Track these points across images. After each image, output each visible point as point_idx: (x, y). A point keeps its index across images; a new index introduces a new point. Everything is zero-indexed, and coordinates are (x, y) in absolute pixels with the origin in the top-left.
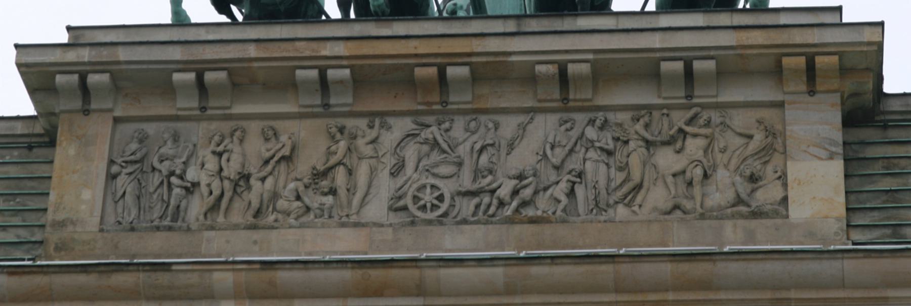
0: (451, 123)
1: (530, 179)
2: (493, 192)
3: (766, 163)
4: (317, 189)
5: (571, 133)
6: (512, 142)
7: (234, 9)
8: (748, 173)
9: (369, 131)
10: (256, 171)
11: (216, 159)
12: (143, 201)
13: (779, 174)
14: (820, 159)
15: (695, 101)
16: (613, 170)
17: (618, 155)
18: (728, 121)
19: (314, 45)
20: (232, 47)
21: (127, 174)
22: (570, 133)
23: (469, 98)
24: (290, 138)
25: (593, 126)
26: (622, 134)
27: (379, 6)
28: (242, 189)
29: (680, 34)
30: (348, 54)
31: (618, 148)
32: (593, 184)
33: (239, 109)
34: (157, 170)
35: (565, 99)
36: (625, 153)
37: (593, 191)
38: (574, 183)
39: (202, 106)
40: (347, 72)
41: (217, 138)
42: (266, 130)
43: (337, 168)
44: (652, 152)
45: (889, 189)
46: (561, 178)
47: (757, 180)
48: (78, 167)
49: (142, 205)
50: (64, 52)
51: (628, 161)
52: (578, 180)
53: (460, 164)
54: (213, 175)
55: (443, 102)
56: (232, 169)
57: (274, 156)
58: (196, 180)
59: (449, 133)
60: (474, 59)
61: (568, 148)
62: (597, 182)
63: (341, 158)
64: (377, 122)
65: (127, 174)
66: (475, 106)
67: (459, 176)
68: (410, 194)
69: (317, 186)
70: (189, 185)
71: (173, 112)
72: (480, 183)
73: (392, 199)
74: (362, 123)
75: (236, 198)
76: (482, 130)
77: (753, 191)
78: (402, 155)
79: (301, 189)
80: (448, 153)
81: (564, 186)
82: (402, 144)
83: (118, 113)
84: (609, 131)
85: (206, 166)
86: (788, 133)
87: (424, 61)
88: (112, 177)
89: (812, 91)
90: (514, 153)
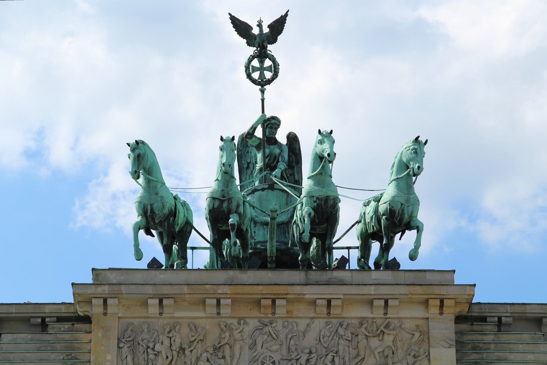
0: (276, 323)
1: (315, 355)
2: (297, 360)
3: (420, 348)
4: (216, 355)
5: (331, 329)
6: (304, 334)
7: (154, 232)
8: (413, 354)
9: (239, 325)
10: (188, 347)
11: (169, 339)
12: (135, 359)
13: (427, 354)
14: (445, 347)
15: (388, 316)
16: (351, 349)
17: (353, 343)
18: (403, 326)
19: (214, 287)
20: (176, 287)
21: (127, 347)
22: (330, 329)
23: (285, 312)
24: (203, 330)
25: (342, 327)
26: (355, 332)
27: (236, 255)
28: (181, 355)
29: (382, 287)
30: (230, 293)
31: (353, 339)
32: (343, 357)
33: (178, 314)
34: (141, 344)
35: (329, 313)
36: (356, 341)
37: (343, 360)
38: (334, 356)
39: (160, 312)
40: (230, 300)
41: (168, 329)
42: (191, 325)
43: (225, 346)
44: (369, 341)
45: (475, 361)
46: (327, 353)
47: (416, 356)
48: (104, 343)
49: (135, 362)
50: (96, 288)
51: (357, 346)
52: (336, 355)
53: (281, 345)
54: (168, 348)
55: (273, 313)
56: (176, 346)
57: (196, 339)
58: (159, 351)
59: (275, 328)
60: (289, 296)
61: (331, 338)
62: (344, 356)
63: (227, 341)
64: (242, 322)
65: (127, 347)
66: (288, 316)
67: (281, 350)
68: (260, 360)
69: (216, 354)
70: (157, 353)
71: (146, 315)
72: (291, 356)
73: (251, 362)
74: (235, 321)
75: (179, 358)
76: (290, 327)
77: (415, 362)
78: (254, 339)
79: (209, 356)
80: (276, 340)
81: (330, 358)
82: (254, 334)
83: (120, 315)
84: (349, 330)
85: (164, 343)
86: (430, 334)
87: (266, 296)
88: (119, 348)
89: (441, 313)
90: (305, 339)
